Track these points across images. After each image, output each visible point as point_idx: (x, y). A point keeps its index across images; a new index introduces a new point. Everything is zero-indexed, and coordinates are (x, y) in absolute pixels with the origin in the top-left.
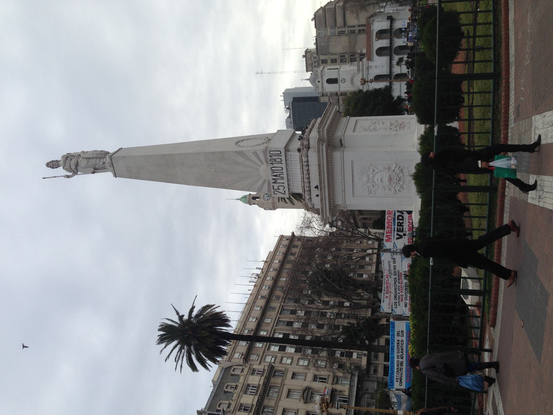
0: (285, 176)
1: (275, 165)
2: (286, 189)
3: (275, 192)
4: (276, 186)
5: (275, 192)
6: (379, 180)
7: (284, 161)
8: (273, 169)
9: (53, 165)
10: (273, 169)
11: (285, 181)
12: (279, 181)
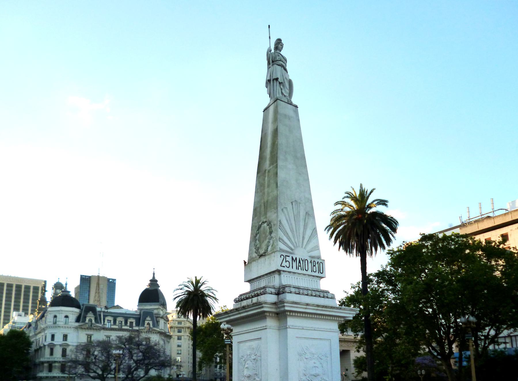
0: (300, 271)
1: (310, 265)
2: (285, 269)
3: (282, 257)
4: (289, 259)
5: (282, 257)
6: (315, 365)
7: (313, 274)
8: (306, 261)
9: (279, 44)
10: (306, 261)
11: (294, 270)
12: (294, 264)
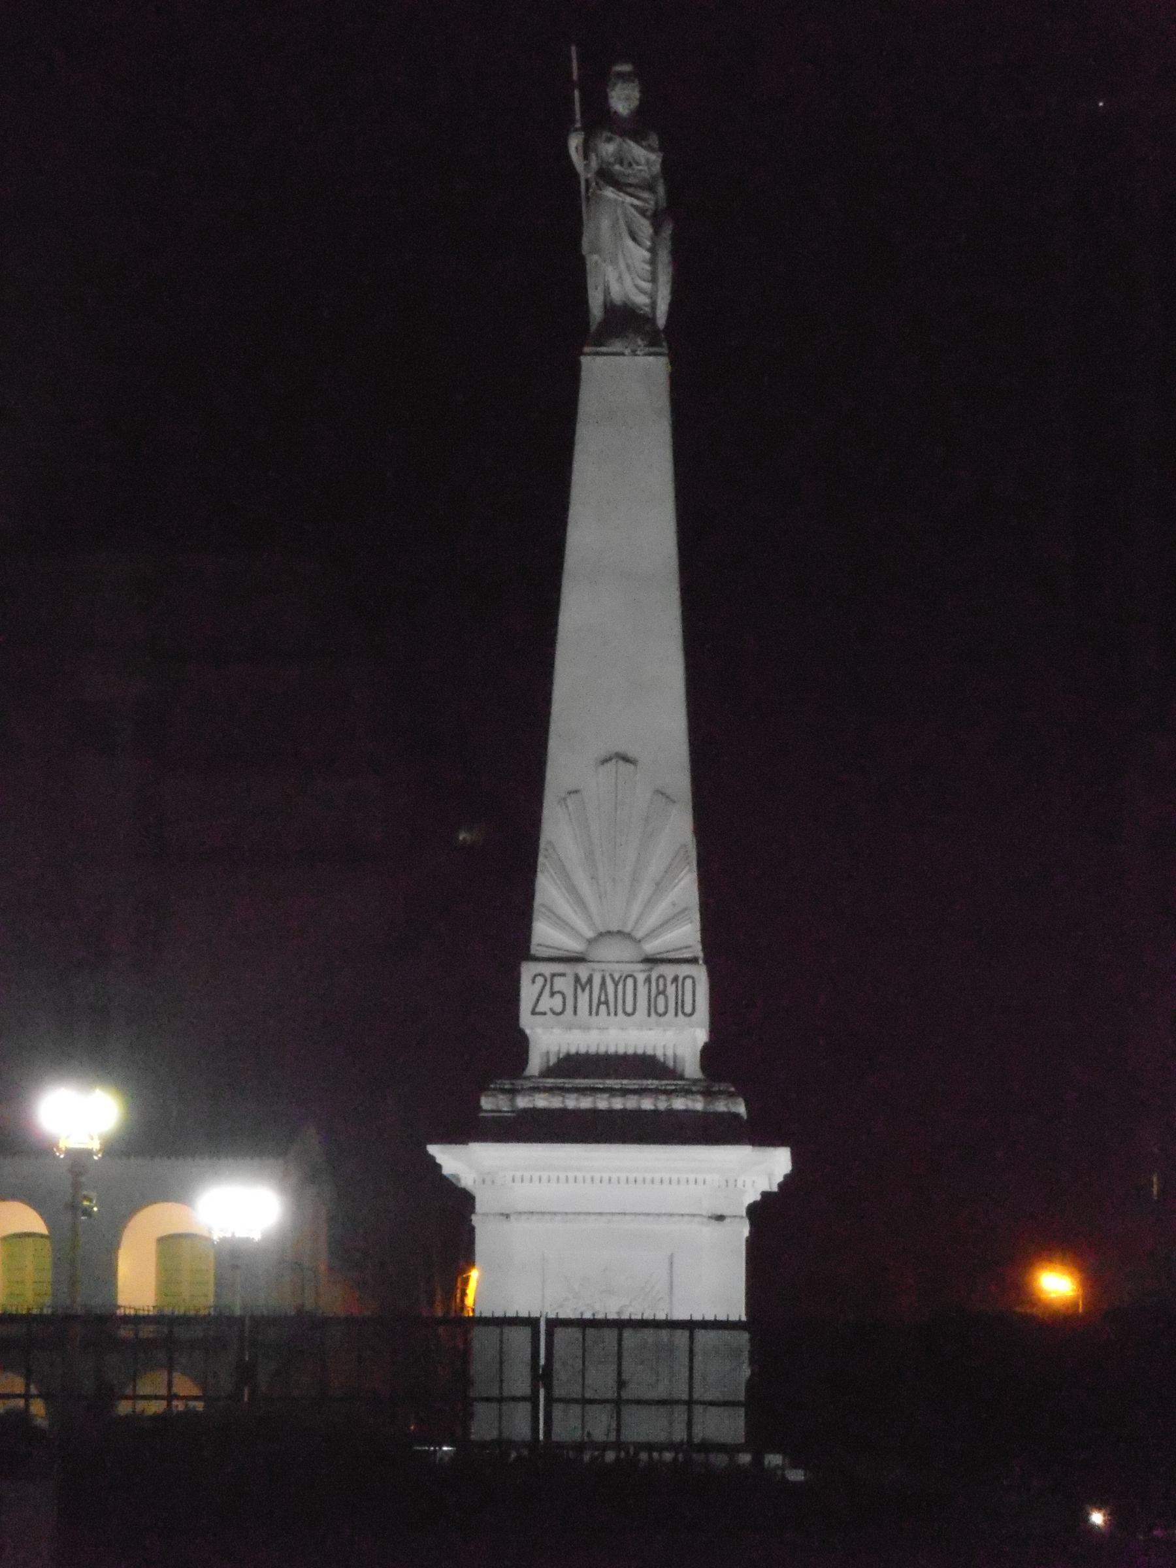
1: (642, 990)
3: (540, 980)
5: (540, 980)
8: (630, 981)
10: (630, 981)
12: (583, 999)
